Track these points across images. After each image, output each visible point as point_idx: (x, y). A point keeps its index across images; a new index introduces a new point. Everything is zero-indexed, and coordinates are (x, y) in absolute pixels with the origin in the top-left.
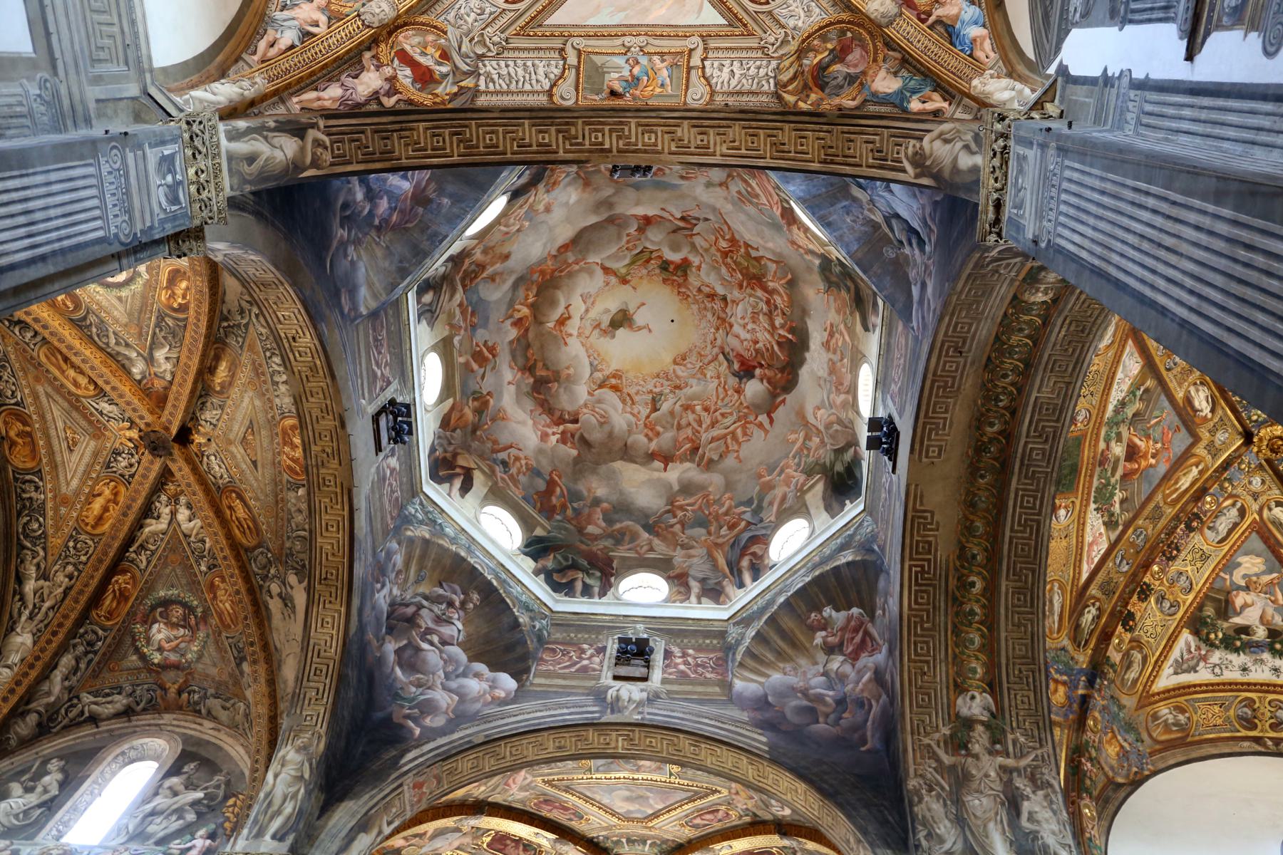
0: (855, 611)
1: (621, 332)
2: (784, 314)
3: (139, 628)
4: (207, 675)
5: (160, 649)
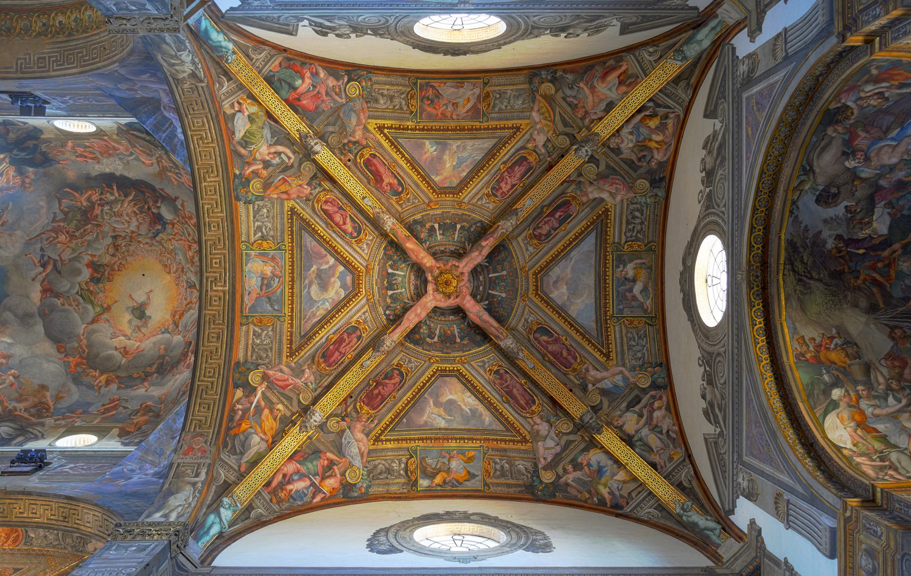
1: (148, 313)
2: (102, 193)
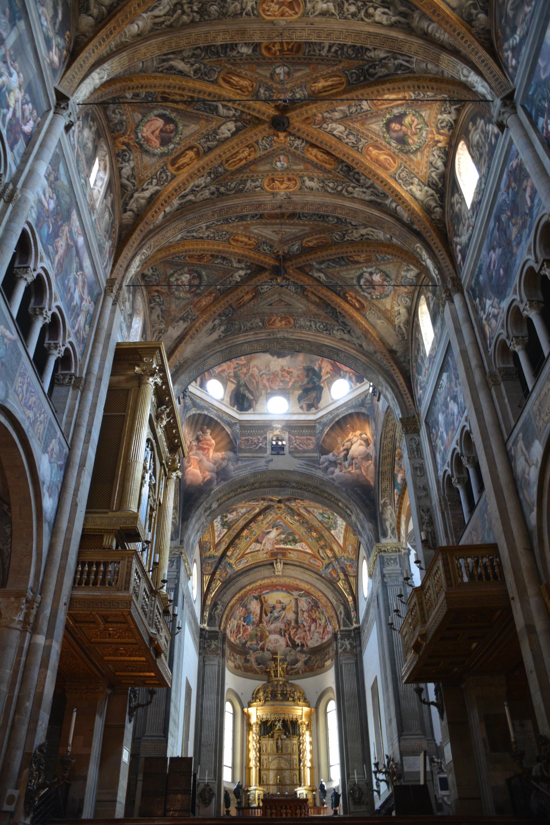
0: (213, 442)
3: (186, 269)
4: (170, 304)
5: (177, 280)
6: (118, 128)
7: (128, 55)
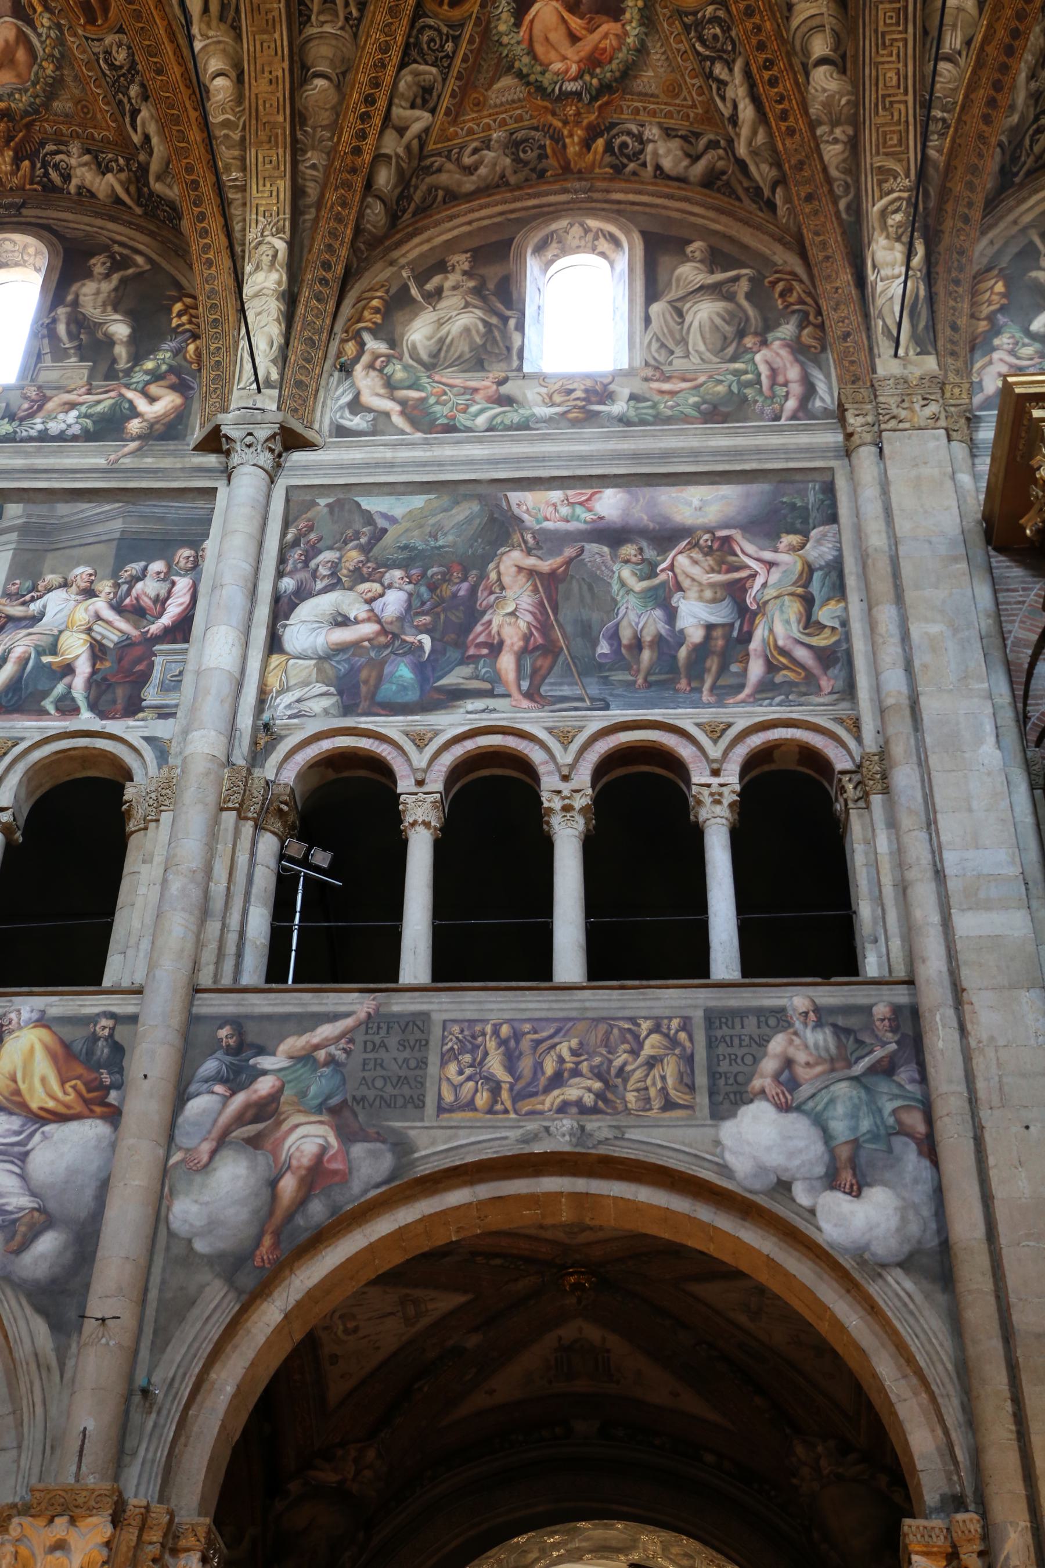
6: (531, 155)
7: (259, 144)
